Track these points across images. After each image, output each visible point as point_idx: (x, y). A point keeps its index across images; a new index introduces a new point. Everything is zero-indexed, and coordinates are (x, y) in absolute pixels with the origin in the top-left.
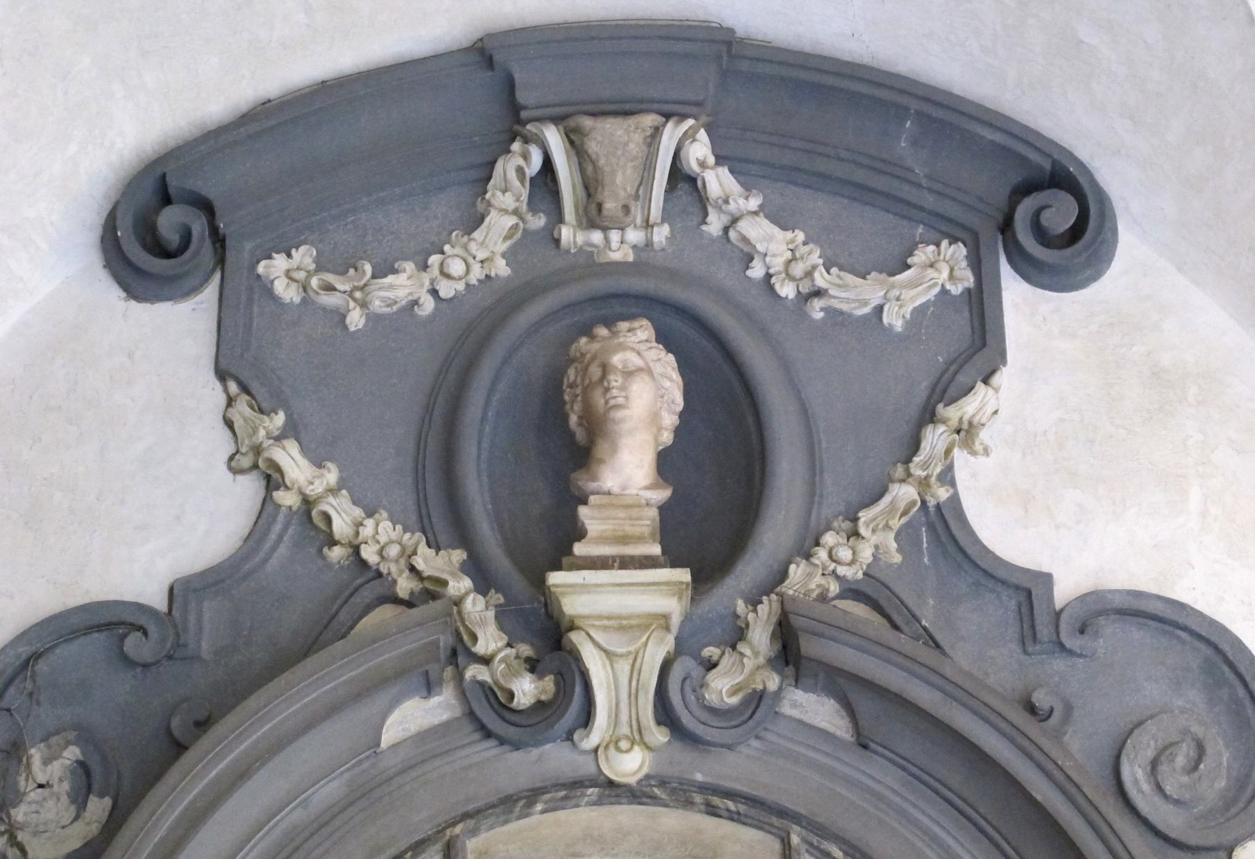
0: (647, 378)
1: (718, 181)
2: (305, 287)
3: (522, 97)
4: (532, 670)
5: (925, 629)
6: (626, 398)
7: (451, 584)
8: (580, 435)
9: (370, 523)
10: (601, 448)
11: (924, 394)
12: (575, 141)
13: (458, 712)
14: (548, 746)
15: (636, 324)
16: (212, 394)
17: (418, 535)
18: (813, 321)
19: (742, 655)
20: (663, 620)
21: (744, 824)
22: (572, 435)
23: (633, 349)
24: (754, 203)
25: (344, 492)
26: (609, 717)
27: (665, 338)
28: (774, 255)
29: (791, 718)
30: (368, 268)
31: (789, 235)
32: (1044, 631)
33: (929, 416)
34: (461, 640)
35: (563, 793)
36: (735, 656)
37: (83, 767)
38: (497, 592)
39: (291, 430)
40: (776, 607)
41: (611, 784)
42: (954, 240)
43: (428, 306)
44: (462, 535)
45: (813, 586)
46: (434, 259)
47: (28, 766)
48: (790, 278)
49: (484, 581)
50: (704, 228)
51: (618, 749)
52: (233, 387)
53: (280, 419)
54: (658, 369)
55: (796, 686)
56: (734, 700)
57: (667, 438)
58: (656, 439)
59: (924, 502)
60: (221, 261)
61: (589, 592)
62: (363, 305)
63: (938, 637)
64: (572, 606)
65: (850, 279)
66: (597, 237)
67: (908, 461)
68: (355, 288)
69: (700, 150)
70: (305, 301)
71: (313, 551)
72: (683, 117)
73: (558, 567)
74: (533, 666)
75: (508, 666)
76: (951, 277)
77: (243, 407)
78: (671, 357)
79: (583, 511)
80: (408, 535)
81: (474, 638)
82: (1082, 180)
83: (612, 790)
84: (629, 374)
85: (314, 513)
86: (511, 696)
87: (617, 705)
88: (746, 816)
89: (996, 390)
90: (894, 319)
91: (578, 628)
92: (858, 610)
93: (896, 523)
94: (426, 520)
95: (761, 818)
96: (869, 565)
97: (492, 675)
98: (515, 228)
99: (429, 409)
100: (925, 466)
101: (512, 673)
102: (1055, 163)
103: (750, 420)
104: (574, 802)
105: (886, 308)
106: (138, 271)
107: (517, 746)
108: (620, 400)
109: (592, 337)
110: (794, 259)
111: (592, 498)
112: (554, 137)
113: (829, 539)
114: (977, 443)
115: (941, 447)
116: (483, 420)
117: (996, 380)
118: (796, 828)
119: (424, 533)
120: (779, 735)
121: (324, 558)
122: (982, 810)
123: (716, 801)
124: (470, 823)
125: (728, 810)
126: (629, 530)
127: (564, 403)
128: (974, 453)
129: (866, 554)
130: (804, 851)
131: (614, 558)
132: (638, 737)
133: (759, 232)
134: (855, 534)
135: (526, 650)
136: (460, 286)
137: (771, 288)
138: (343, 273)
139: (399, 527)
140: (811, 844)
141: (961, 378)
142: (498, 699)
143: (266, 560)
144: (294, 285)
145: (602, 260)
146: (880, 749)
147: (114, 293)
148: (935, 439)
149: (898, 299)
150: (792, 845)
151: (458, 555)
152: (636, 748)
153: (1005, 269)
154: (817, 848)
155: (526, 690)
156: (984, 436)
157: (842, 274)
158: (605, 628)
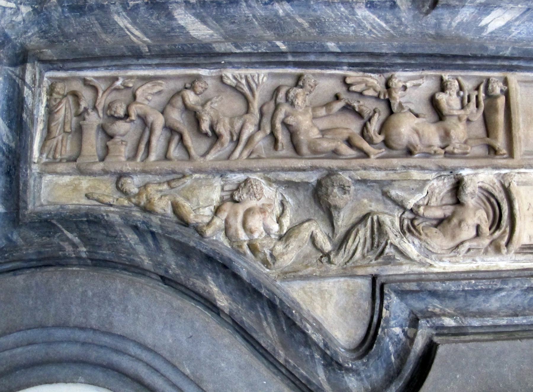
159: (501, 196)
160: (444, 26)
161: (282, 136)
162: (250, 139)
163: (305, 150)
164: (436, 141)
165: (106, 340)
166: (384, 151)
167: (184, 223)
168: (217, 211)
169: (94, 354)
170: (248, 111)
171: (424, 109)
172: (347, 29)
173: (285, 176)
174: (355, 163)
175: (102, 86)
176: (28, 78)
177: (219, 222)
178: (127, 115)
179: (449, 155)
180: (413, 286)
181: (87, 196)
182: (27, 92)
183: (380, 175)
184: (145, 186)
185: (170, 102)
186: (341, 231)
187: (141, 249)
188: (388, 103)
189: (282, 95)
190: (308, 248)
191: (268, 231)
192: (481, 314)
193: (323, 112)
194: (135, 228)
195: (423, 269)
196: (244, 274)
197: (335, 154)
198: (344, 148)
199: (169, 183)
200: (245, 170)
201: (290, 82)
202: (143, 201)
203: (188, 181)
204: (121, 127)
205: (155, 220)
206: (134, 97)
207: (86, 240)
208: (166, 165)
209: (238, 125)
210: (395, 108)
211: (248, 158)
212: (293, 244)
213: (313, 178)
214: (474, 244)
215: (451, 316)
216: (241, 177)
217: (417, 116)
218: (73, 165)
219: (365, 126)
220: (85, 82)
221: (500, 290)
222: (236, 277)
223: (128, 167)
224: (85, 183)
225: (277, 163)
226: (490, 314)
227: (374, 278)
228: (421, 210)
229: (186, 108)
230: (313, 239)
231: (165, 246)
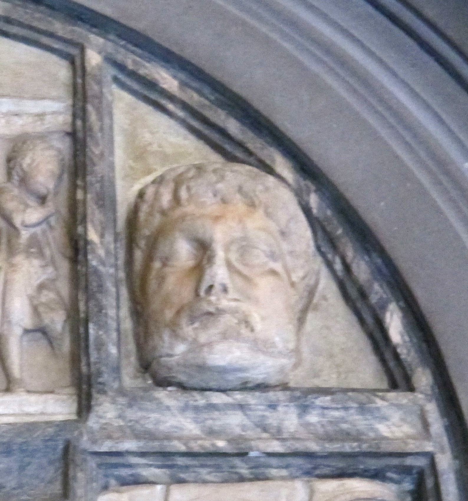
95: (35, 24)
122: (430, 12)
130: (109, 78)
140: (121, 67)
150: (89, 69)
154: (133, 75)
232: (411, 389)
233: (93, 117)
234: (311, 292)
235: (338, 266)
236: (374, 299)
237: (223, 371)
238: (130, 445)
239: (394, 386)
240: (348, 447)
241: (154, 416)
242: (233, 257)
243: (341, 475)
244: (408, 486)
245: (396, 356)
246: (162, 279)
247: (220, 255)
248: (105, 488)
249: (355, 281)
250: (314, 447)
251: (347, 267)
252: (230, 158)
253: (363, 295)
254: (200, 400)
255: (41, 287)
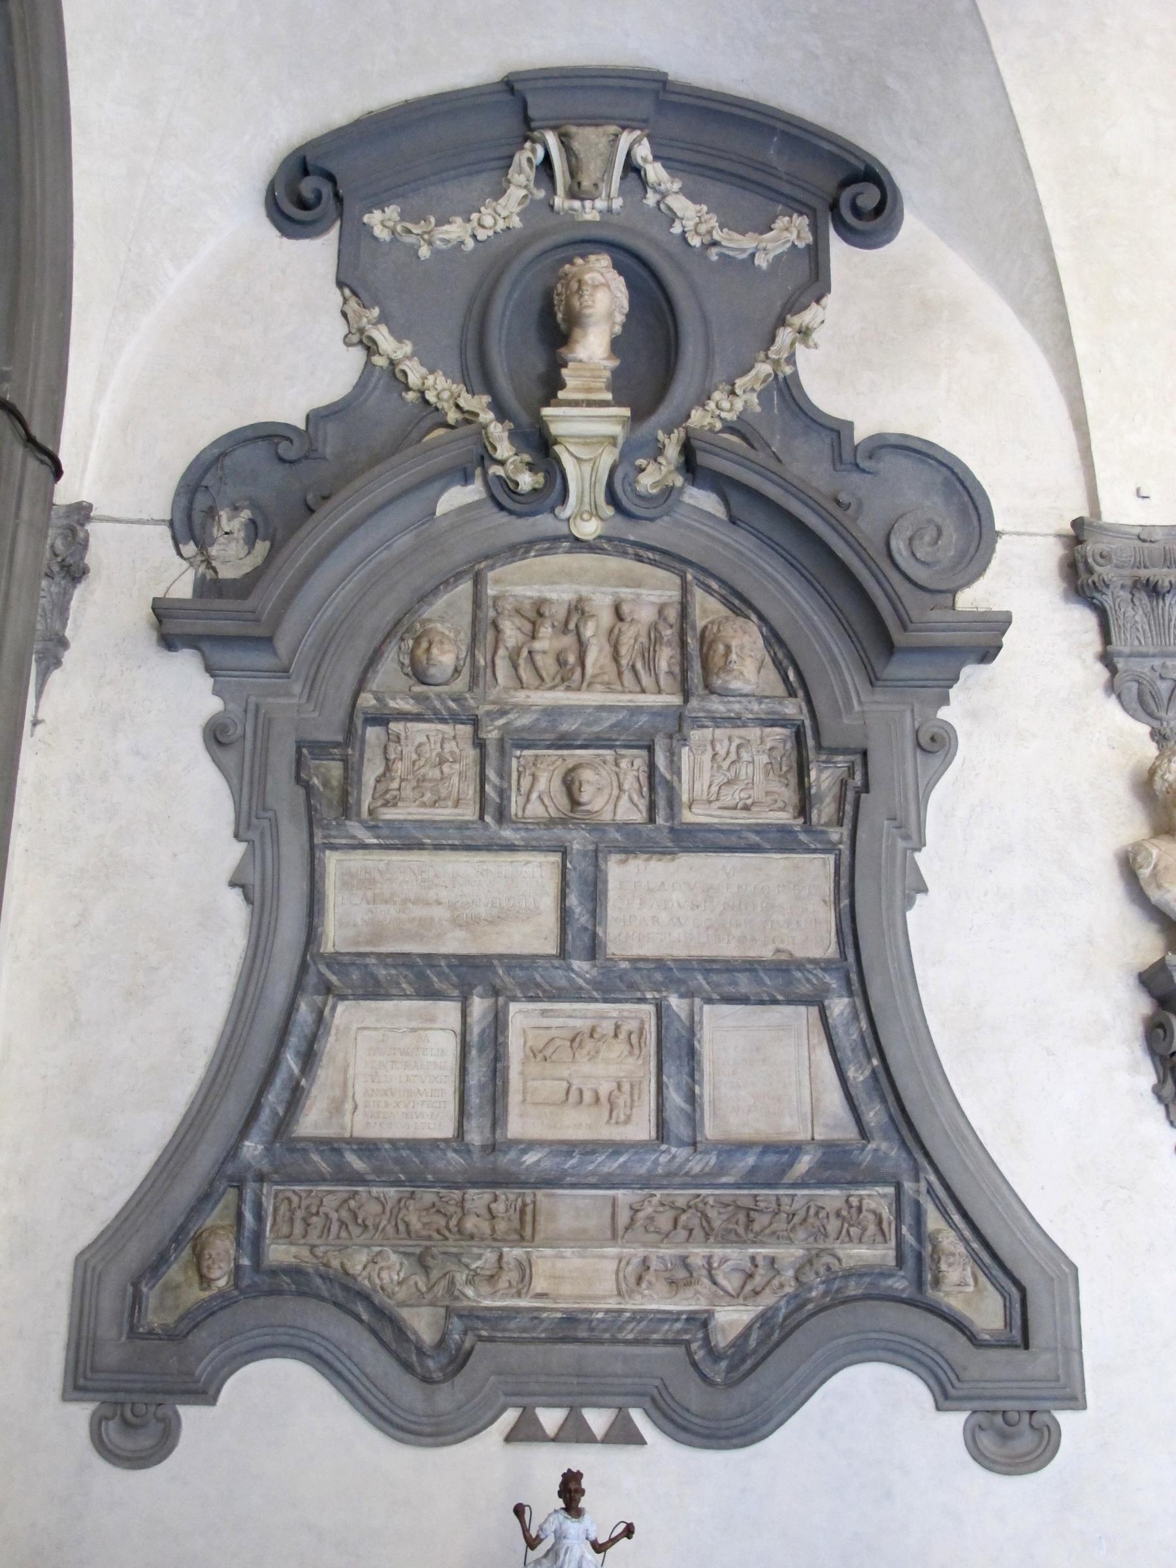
0: (606, 290)
1: (655, 172)
2: (393, 232)
3: (531, 112)
4: (530, 470)
5: (774, 453)
6: (594, 301)
7: (481, 415)
8: (563, 327)
9: (431, 378)
10: (577, 333)
11: (779, 309)
12: (565, 140)
13: (484, 495)
14: (538, 517)
15: (600, 257)
16: (335, 297)
17: (462, 386)
18: (711, 262)
19: (660, 463)
20: (613, 440)
21: (659, 567)
22: (557, 326)
23: (598, 272)
24: (677, 186)
25: (416, 358)
26: (577, 499)
27: (618, 266)
28: (688, 219)
29: (689, 504)
30: (433, 220)
31: (698, 207)
32: (847, 456)
33: (782, 322)
34: (487, 450)
35: (547, 545)
36: (656, 465)
37: (252, 522)
38: (510, 421)
39: (383, 319)
40: (683, 434)
41: (577, 539)
42: (801, 214)
43: (470, 244)
44: (489, 386)
45: (705, 423)
46: (474, 216)
47: (219, 520)
48: (698, 234)
49: (502, 413)
50: (645, 201)
51: (582, 519)
52: (347, 292)
53: (376, 312)
54: (613, 285)
55: (693, 485)
56: (654, 491)
57: (618, 329)
58: (611, 331)
59: (776, 376)
60: (341, 215)
61: (567, 421)
62: (430, 243)
63: (781, 457)
64: (556, 429)
65: (736, 236)
66: (577, 204)
67: (768, 349)
68: (425, 233)
69: (643, 151)
70: (392, 240)
71: (395, 395)
72: (634, 129)
73: (548, 405)
74: (531, 467)
75: (516, 467)
76: (798, 237)
77: (353, 303)
78: (622, 279)
79: (564, 371)
80: (455, 386)
81: (495, 449)
82: (884, 178)
83: (579, 545)
84: (595, 287)
85: (397, 370)
86: (517, 484)
87: (582, 493)
88: (661, 563)
89: (824, 308)
90: (762, 261)
91: (560, 443)
92: (734, 439)
93: (758, 387)
94: (466, 378)
96: (740, 413)
97: (506, 472)
98: (525, 197)
99: (469, 310)
100: (778, 352)
101: (517, 470)
102: (867, 166)
103: (670, 321)
104: (554, 551)
105: (757, 255)
106: (289, 219)
107: (519, 515)
108: (590, 303)
109: (572, 263)
110: (700, 222)
111: (570, 364)
112: (551, 139)
113: (717, 395)
114: (810, 340)
115: (788, 341)
116: (503, 315)
117: (824, 301)
118: (690, 570)
119: (465, 385)
120: (683, 515)
121: (403, 399)
123: (641, 552)
124: (490, 562)
125: (649, 558)
126: (593, 385)
127: (554, 305)
128: (808, 346)
129: (739, 405)
131: (583, 401)
132: (595, 512)
133: (680, 204)
134: (733, 393)
135: (527, 458)
136: (491, 233)
137: (685, 240)
138: (417, 223)
139: (449, 381)
140: (698, 580)
141: (802, 300)
142: (509, 487)
143: (366, 400)
144: (386, 230)
145: (580, 219)
146: (743, 525)
147: (274, 233)
148: (785, 336)
149: (765, 249)
151: (486, 399)
152: (593, 519)
153: (833, 234)
154: (703, 583)
155: (527, 481)
156: (815, 336)
157: (730, 232)
158: (576, 444)
159: (526, 1264)
160: (499, 1162)
161: (402, 1227)
162: (384, 1229)
163: (413, 1235)
164: (488, 1231)
165: (304, 1334)
166: (458, 1237)
167: (346, 1273)
168: (365, 1267)
169: (296, 1342)
170: (384, 1212)
171: (484, 1212)
172: (441, 1165)
173: (402, 1249)
174: (440, 1243)
175: (304, 1195)
176: (265, 1191)
177: (365, 1273)
178: (317, 1213)
179: (495, 1240)
180: (466, 1313)
181: (294, 1257)
182: (264, 1199)
183: (454, 1250)
184: (325, 1253)
185: (341, 1206)
186: (433, 1281)
187: (323, 1287)
188: (463, 1208)
189: (402, 1204)
190: (414, 1290)
191: (392, 1280)
192: (504, 1330)
193: (424, 1213)
194: (321, 1276)
195: (474, 1304)
196: (376, 1301)
197: (430, 1238)
198: (435, 1235)
199: (339, 1250)
200: (380, 1246)
201: (408, 1195)
202: (325, 1261)
203: (350, 1250)
204: (314, 1219)
205: (331, 1272)
206: (322, 1202)
207: (294, 1282)
208: (339, 1242)
209: (377, 1220)
210: (466, 1212)
211: (383, 1239)
212: (404, 1287)
213: (418, 1251)
214: (506, 1291)
215: (486, 1330)
216: (378, 1249)
217: (478, 1216)
218: (287, 1240)
219: (447, 1223)
220: (294, 1192)
221: (515, 1318)
222: (372, 1303)
223: (318, 1242)
224: (293, 1249)
225: (398, 1242)
226: (509, 1330)
227: (447, 1308)
228: (479, 1270)
229: (350, 1210)
230: (416, 1284)
231: (337, 1286)
232: (796, 696)
233: (689, 598)
234: (763, 662)
235: (772, 653)
236: (784, 665)
237: (734, 690)
238: (701, 715)
239: (790, 695)
240: (775, 717)
241: (710, 704)
242: (738, 650)
243: (772, 726)
244: (794, 730)
245: (792, 686)
246: (713, 658)
247: (734, 650)
248: (693, 729)
249: (777, 658)
250: (763, 716)
251: (775, 654)
252: (737, 615)
253: (781, 664)
254: (725, 699)
255: (671, 657)
